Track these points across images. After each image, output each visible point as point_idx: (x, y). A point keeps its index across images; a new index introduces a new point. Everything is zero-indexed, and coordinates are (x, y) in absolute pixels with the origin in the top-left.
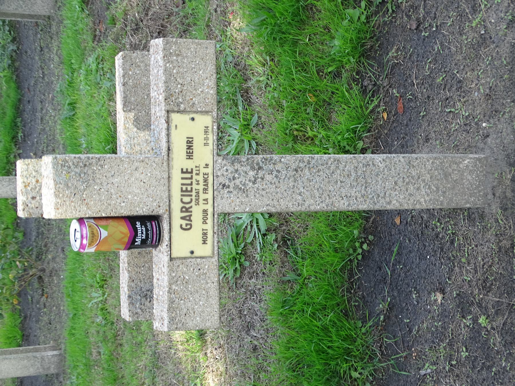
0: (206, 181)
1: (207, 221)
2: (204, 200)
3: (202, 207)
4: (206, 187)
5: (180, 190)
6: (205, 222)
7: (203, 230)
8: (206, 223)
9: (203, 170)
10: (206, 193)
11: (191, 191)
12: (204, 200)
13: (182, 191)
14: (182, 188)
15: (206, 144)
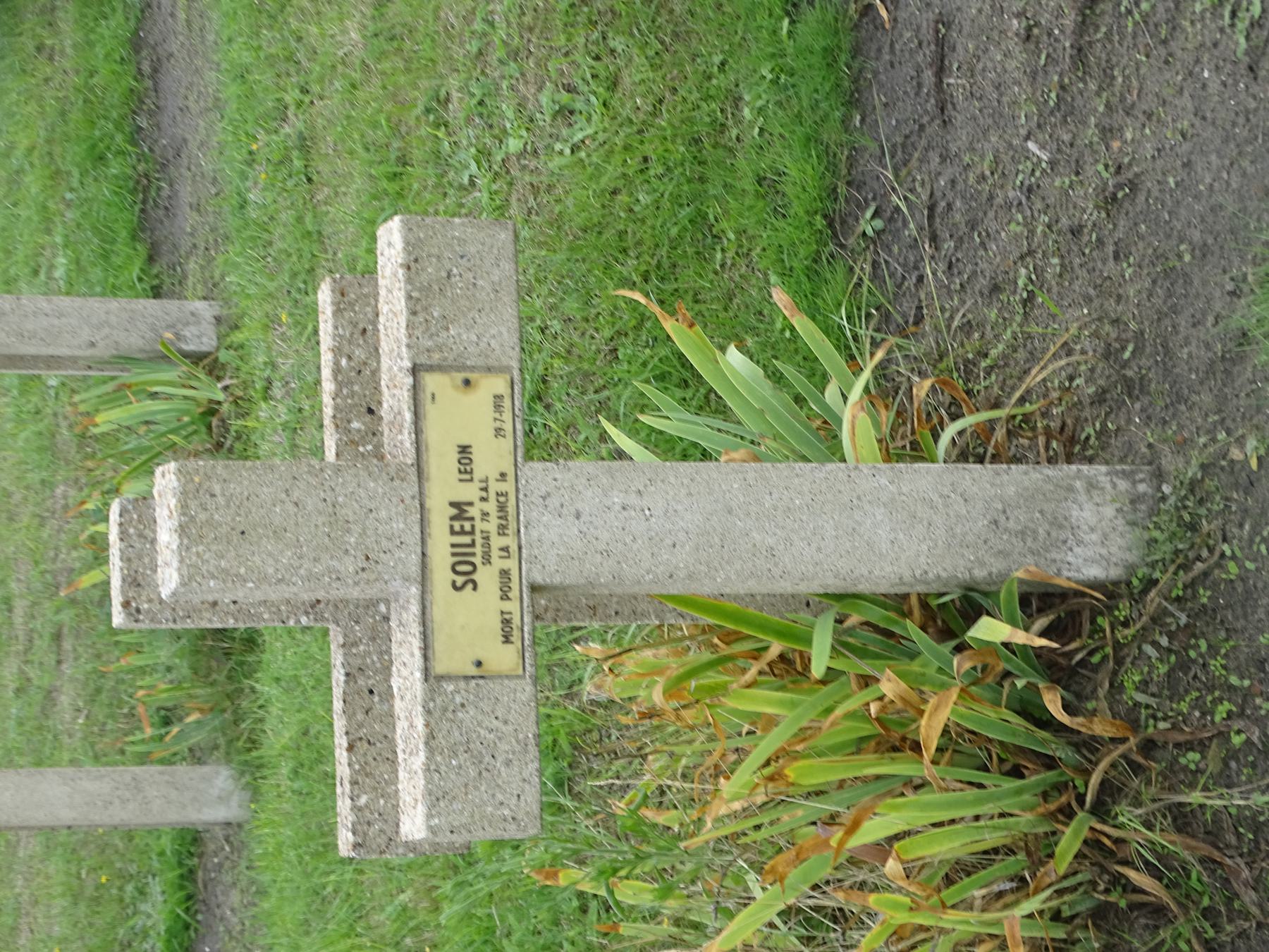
0: (502, 508)
1: (510, 595)
2: (502, 549)
3: (498, 563)
4: (504, 522)
5: (447, 530)
6: (505, 597)
7: (502, 612)
8: (509, 599)
9: (494, 487)
10: (504, 534)
11: (472, 532)
12: (502, 549)
13: (453, 532)
14: (452, 527)
15: (499, 432)
